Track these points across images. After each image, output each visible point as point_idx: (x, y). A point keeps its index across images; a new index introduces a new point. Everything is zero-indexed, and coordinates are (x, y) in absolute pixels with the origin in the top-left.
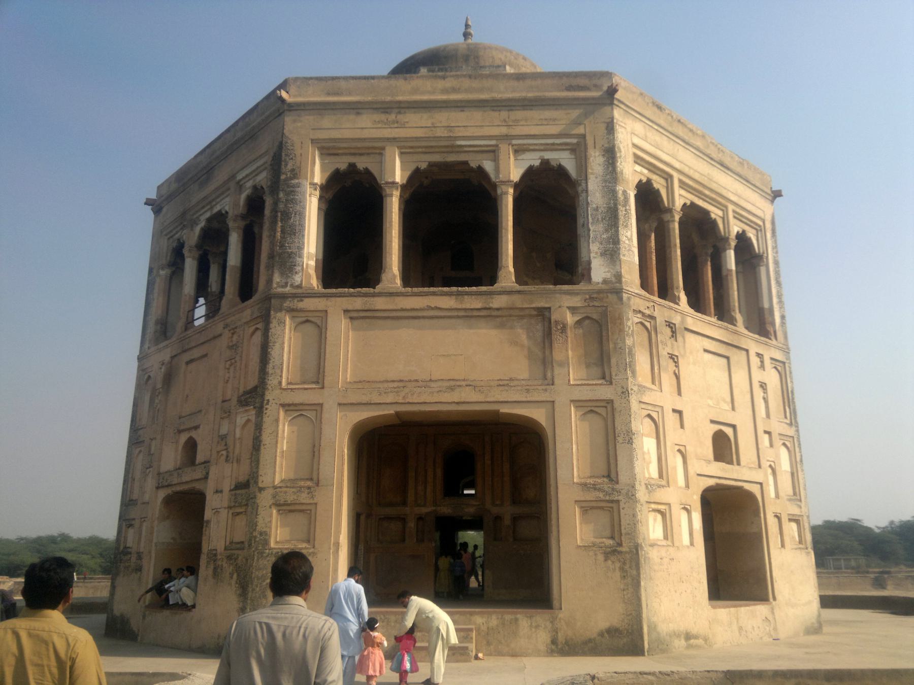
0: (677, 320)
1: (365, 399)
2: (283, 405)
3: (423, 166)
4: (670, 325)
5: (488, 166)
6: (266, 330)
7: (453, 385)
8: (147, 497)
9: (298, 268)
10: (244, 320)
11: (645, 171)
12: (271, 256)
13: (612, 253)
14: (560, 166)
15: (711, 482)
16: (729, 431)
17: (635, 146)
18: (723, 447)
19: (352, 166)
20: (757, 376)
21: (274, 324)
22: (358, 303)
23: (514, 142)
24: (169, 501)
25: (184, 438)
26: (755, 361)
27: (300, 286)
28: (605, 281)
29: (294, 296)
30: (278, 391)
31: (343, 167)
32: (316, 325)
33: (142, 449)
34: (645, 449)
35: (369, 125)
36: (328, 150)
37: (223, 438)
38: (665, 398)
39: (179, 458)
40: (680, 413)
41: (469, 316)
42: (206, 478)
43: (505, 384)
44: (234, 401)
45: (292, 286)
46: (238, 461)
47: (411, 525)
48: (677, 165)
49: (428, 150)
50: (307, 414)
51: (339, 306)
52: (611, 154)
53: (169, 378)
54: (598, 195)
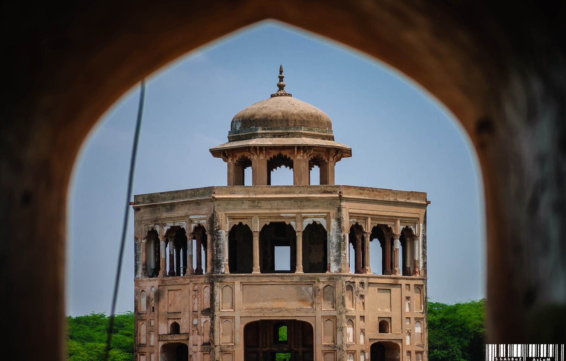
0: (365, 280)
1: (249, 315)
2: (221, 317)
3: (268, 224)
4: (362, 284)
5: (293, 224)
6: (212, 290)
8: (152, 344)
9: (223, 266)
10: (200, 282)
11: (355, 220)
12: (213, 260)
13: (338, 261)
14: (320, 224)
15: (376, 341)
16: (388, 320)
17: (349, 213)
18: (383, 326)
19: (241, 223)
21: (216, 287)
22: (245, 280)
23: (303, 215)
24: (164, 347)
25: (171, 322)
27: (223, 273)
28: (335, 272)
29: (222, 276)
30: (219, 312)
31: (237, 224)
33: (145, 323)
34: (348, 332)
35: (247, 207)
36: (232, 217)
37: (196, 325)
39: (169, 329)
40: (364, 317)
41: (286, 284)
42: (188, 339)
43: (298, 310)
44: (199, 312)
45: (221, 273)
46: (203, 335)
48: (371, 213)
49: (270, 217)
53: (158, 295)
54: (334, 238)
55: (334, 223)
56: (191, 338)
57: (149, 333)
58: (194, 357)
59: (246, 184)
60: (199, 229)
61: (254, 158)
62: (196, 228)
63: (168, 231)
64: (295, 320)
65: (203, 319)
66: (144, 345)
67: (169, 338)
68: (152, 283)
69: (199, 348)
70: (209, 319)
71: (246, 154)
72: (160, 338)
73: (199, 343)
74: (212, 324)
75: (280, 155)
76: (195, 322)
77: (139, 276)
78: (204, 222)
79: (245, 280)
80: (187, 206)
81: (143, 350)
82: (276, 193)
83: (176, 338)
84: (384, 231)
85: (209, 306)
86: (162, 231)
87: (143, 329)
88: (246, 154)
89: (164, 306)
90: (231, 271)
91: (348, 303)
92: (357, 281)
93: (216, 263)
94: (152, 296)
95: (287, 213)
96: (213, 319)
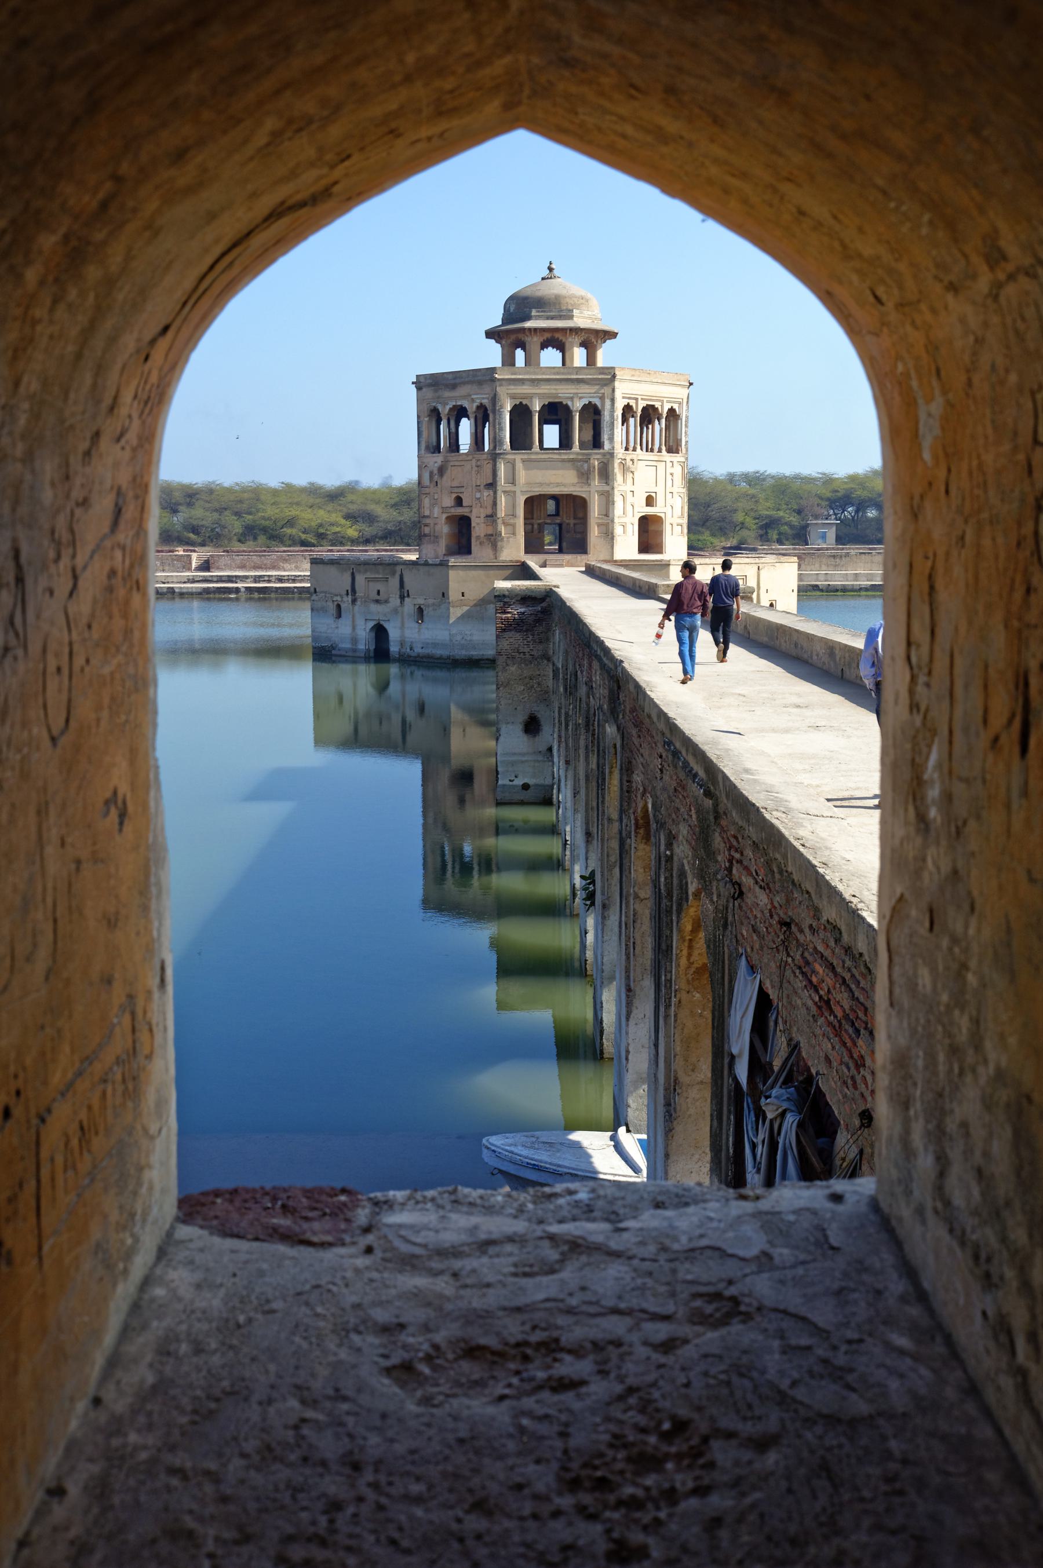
5: (570, 404)
7: (558, 485)
13: (611, 439)
16: (654, 495)
18: (650, 501)
20: (669, 470)
22: (526, 457)
24: (447, 518)
25: (454, 496)
26: (669, 465)
32: (513, 464)
36: (513, 397)
38: (629, 487)
44: (482, 487)
47: (536, 526)
50: (511, 495)
51: (519, 457)
52: (613, 400)
53: (442, 470)
55: (608, 403)
56: (475, 511)
57: (432, 505)
58: (477, 528)
59: (517, 365)
60: (482, 407)
61: (528, 339)
62: (478, 407)
63: (451, 409)
64: (570, 495)
65: (486, 494)
66: (428, 517)
67: (453, 510)
68: (435, 459)
69: (482, 519)
70: (491, 493)
71: (521, 336)
72: (444, 510)
73: (483, 516)
74: (495, 498)
75: (553, 337)
76: (478, 495)
77: (423, 452)
78: (485, 402)
79: (526, 457)
80: (469, 386)
81: (427, 521)
82: (554, 374)
83: (460, 511)
84: (651, 411)
85: (490, 481)
86: (444, 410)
87: (426, 502)
88: (521, 336)
89: (446, 481)
90: (512, 448)
91: (619, 477)
92: (628, 460)
93: (496, 441)
94: (436, 472)
95: (563, 393)
96: (495, 493)
